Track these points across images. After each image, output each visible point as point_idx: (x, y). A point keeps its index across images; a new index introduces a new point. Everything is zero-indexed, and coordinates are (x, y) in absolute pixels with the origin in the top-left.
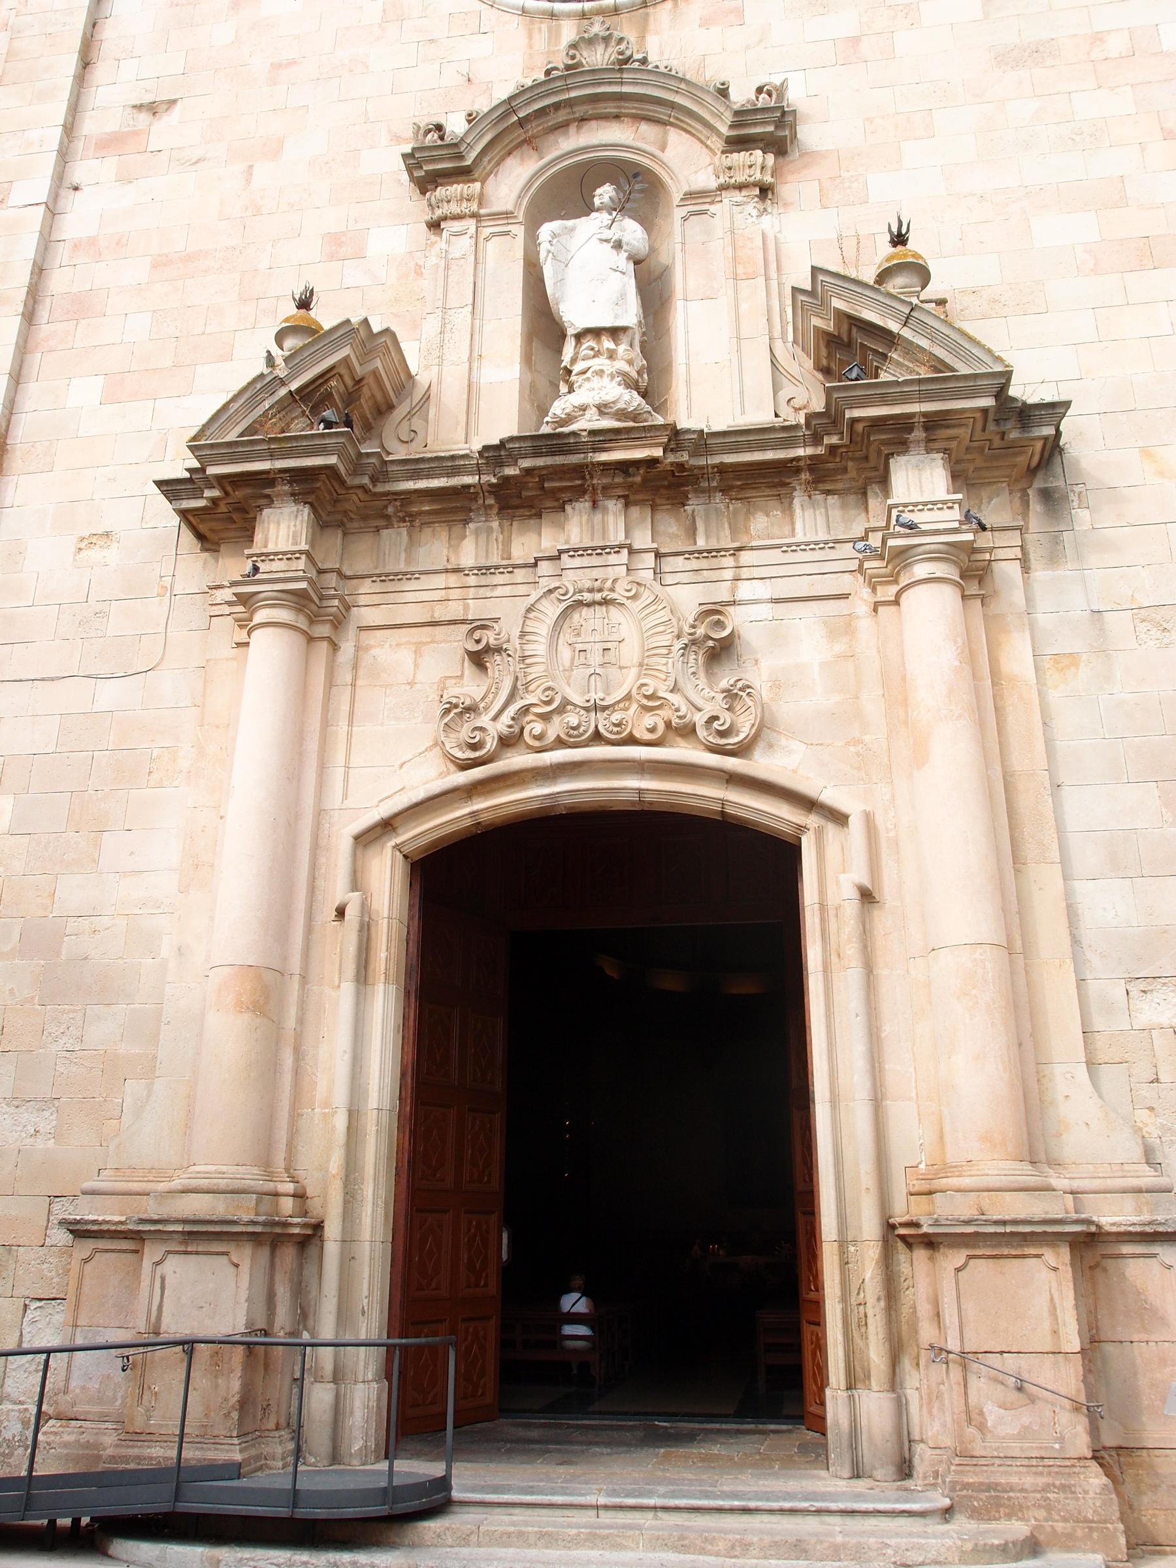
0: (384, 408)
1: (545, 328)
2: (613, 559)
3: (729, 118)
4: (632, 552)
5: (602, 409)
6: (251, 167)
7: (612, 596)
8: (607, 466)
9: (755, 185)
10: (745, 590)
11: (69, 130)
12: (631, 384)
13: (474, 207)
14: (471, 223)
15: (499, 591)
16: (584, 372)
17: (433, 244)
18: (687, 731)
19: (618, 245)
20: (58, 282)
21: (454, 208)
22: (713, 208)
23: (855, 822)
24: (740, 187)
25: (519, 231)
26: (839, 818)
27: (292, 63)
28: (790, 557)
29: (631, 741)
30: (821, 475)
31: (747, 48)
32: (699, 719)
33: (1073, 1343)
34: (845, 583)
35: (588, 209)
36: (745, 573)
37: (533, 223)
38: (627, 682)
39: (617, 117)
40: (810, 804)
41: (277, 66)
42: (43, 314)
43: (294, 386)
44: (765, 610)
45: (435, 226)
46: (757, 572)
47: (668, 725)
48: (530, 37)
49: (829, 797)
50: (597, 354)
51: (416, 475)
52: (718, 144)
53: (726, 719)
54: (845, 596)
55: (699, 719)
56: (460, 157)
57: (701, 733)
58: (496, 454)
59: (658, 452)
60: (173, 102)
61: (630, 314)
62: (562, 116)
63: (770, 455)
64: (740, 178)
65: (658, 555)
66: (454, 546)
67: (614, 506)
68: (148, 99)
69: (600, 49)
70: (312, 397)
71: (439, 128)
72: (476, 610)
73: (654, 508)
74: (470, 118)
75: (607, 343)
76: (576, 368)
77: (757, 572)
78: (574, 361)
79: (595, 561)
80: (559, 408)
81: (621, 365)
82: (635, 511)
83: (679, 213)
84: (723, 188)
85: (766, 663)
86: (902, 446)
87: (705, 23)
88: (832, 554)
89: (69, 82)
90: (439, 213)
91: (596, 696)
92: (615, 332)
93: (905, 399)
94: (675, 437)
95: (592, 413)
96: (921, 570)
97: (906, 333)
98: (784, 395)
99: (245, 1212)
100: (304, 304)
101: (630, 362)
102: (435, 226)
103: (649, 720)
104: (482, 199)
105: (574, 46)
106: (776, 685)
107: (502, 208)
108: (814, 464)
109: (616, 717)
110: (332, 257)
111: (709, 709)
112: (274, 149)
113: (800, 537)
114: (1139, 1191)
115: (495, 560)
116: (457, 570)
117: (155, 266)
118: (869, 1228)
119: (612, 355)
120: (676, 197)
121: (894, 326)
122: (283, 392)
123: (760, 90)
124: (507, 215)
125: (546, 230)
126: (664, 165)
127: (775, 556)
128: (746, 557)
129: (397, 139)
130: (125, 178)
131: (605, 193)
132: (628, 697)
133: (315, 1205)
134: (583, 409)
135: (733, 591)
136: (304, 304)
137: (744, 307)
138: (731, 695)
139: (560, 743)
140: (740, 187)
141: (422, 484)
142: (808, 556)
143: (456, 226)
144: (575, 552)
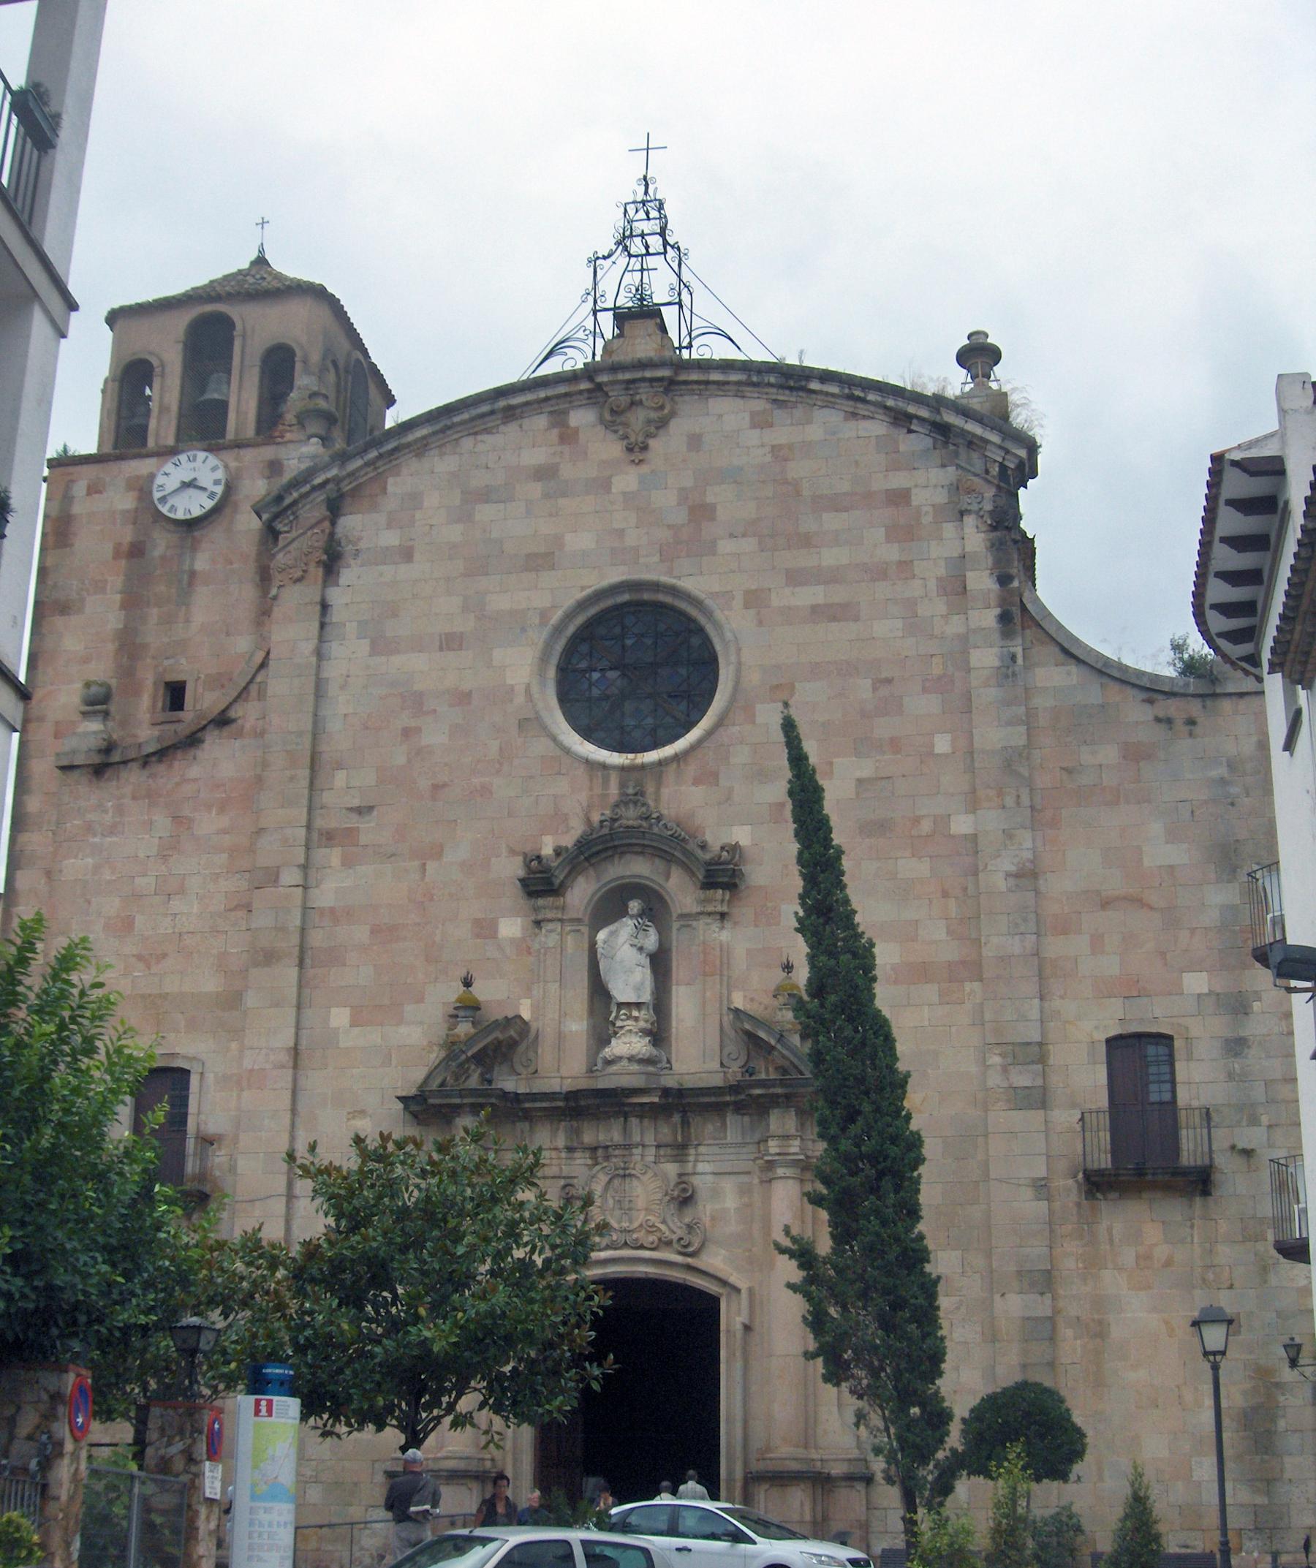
0: (513, 1044)
1: (599, 991)
2: (635, 1151)
3: (702, 871)
4: (643, 1146)
5: (631, 1059)
6: (424, 864)
7: (633, 1172)
8: (630, 1104)
9: (716, 913)
10: (701, 1167)
11: (309, 827)
12: (646, 1032)
13: (560, 916)
14: (558, 926)
15: (578, 1162)
16: (622, 1027)
17: (536, 935)
18: (669, 1243)
19: (641, 949)
20: (317, 938)
21: (550, 915)
22: (694, 923)
23: (744, 1294)
24: (709, 914)
25: (585, 929)
26: (738, 1290)
27: (445, 785)
28: (722, 1151)
29: (642, 1247)
30: (739, 1108)
31: (720, 803)
32: (675, 1237)
33: (808, 1517)
34: (748, 1166)
35: (623, 912)
36: (701, 1158)
37: (595, 929)
38: (640, 1218)
39: (642, 853)
40: (724, 1283)
41: (436, 787)
42: (308, 961)
43: (469, 1054)
44: (710, 1178)
45: (538, 923)
46: (707, 1158)
47: (660, 1240)
48: (591, 780)
49: (733, 1279)
50: (629, 1017)
51: (534, 1100)
52: (699, 885)
53: (686, 1239)
54: (749, 1173)
55: (675, 1237)
56: (551, 884)
57: (675, 1245)
58: (572, 1096)
59: (656, 1100)
60: (371, 808)
61: (646, 997)
62: (610, 853)
63: (713, 1099)
64: (710, 909)
65: (658, 1147)
66: (554, 1133)
67: (634, 1121)
68: (356, 802)
69: (631, 805)
70: (479, 1058)
71: (539, 858)
72: (566, 1171)
73: (656, 1119)
74: (558, 851)
75: (635, 1013)
76: (619, 1023)
77: (707, 1158)
78: (616, 1018)
79: (626, 1152)
80: (607, 1052)
81: (642, 1024)
82: (646, 1122)
83: (675, 925)
84: (701, 913)
85: (708, 1207)
86: (777, 1105)
87: (697, 782)
88: (745, 1150)
89: (306, 792)
90: (540, 917)
91: (625, 1225)
92: (638, 1005)
93: (774, 1086)
94: (666, 1092)
95: (625, 1062)
96: (780, 1171)
97: (779, 1047)
98: (726, 1052)
99: (473, 1466)
100: (467, 983)
101: (646, 1021)
102: (538, 923)
103: (651, 1238)
104: (563, 908)
105: (617, 806)
106: (713, 1219)
107: (575, 916)
108: (735, 1103)
109: (635, 1236)
110: (478, 936)
111: (680, 1233)
112: (437, 852)
113: (729, 1140)
114: (849, 1460)
115: (575, 1145)
116: (556, 1149)
117: (372, 933)
118: (739, 1474)
119: (636, 1019)
120: (675, 915)
121: (773, 1042)
122: (463, 1057)
123: (722, 848)
124: (579, 921)
125: (601, 936)
126: (668, 893)
127: (716, 1149)
128: (702, 1149)
129: (513, 852)
130: (348, 863)
131: (634, 906)
132: (641, 1225)
133: (499, 1464)
134: (621, 1058)
135: (695, 1166)
136: (467, 983)
137: (708, 994)
138: (690, 1227)
139: (608, 1247)
140: (709, 914)
141: (538, 1105)
142: (732, 1150)
143: (550, 926)
144: (617, 1147)
